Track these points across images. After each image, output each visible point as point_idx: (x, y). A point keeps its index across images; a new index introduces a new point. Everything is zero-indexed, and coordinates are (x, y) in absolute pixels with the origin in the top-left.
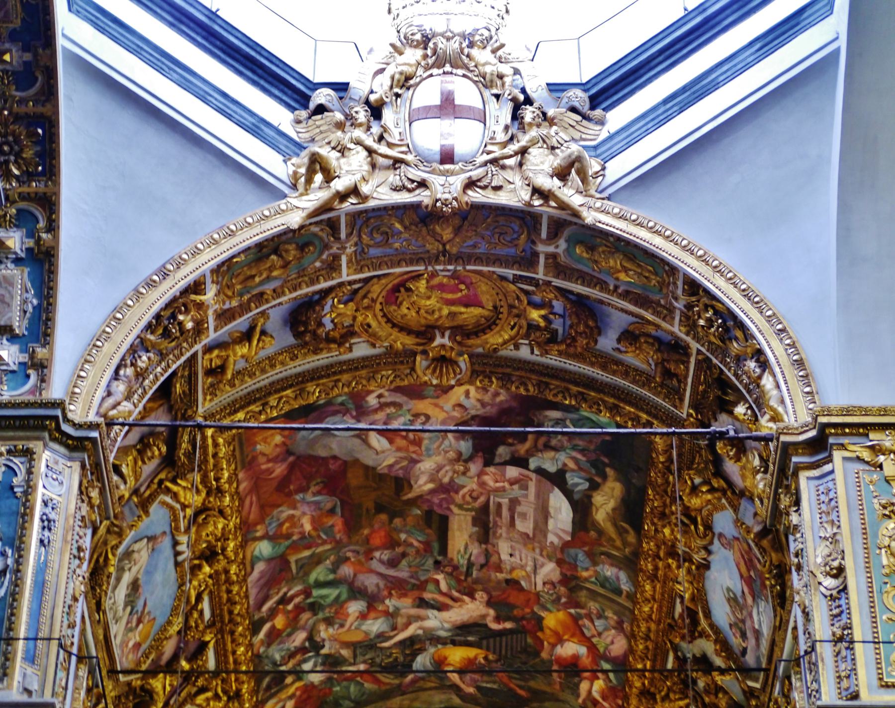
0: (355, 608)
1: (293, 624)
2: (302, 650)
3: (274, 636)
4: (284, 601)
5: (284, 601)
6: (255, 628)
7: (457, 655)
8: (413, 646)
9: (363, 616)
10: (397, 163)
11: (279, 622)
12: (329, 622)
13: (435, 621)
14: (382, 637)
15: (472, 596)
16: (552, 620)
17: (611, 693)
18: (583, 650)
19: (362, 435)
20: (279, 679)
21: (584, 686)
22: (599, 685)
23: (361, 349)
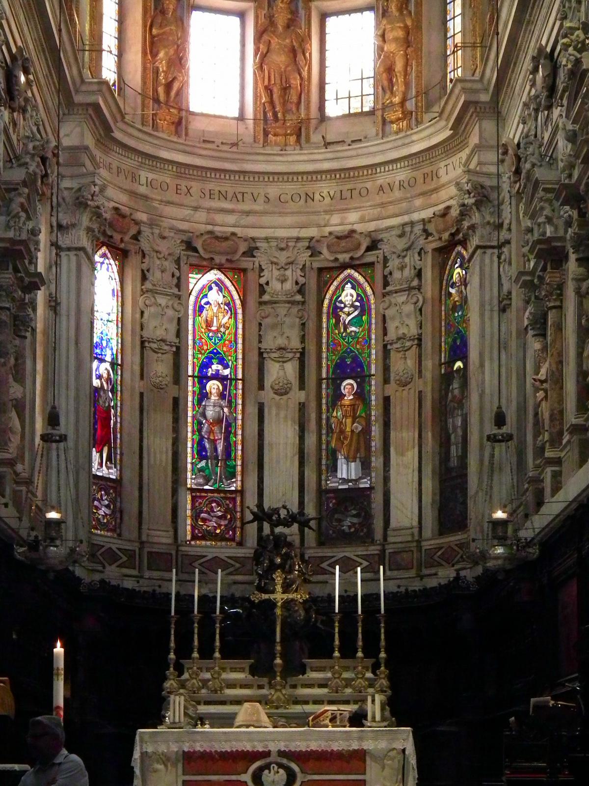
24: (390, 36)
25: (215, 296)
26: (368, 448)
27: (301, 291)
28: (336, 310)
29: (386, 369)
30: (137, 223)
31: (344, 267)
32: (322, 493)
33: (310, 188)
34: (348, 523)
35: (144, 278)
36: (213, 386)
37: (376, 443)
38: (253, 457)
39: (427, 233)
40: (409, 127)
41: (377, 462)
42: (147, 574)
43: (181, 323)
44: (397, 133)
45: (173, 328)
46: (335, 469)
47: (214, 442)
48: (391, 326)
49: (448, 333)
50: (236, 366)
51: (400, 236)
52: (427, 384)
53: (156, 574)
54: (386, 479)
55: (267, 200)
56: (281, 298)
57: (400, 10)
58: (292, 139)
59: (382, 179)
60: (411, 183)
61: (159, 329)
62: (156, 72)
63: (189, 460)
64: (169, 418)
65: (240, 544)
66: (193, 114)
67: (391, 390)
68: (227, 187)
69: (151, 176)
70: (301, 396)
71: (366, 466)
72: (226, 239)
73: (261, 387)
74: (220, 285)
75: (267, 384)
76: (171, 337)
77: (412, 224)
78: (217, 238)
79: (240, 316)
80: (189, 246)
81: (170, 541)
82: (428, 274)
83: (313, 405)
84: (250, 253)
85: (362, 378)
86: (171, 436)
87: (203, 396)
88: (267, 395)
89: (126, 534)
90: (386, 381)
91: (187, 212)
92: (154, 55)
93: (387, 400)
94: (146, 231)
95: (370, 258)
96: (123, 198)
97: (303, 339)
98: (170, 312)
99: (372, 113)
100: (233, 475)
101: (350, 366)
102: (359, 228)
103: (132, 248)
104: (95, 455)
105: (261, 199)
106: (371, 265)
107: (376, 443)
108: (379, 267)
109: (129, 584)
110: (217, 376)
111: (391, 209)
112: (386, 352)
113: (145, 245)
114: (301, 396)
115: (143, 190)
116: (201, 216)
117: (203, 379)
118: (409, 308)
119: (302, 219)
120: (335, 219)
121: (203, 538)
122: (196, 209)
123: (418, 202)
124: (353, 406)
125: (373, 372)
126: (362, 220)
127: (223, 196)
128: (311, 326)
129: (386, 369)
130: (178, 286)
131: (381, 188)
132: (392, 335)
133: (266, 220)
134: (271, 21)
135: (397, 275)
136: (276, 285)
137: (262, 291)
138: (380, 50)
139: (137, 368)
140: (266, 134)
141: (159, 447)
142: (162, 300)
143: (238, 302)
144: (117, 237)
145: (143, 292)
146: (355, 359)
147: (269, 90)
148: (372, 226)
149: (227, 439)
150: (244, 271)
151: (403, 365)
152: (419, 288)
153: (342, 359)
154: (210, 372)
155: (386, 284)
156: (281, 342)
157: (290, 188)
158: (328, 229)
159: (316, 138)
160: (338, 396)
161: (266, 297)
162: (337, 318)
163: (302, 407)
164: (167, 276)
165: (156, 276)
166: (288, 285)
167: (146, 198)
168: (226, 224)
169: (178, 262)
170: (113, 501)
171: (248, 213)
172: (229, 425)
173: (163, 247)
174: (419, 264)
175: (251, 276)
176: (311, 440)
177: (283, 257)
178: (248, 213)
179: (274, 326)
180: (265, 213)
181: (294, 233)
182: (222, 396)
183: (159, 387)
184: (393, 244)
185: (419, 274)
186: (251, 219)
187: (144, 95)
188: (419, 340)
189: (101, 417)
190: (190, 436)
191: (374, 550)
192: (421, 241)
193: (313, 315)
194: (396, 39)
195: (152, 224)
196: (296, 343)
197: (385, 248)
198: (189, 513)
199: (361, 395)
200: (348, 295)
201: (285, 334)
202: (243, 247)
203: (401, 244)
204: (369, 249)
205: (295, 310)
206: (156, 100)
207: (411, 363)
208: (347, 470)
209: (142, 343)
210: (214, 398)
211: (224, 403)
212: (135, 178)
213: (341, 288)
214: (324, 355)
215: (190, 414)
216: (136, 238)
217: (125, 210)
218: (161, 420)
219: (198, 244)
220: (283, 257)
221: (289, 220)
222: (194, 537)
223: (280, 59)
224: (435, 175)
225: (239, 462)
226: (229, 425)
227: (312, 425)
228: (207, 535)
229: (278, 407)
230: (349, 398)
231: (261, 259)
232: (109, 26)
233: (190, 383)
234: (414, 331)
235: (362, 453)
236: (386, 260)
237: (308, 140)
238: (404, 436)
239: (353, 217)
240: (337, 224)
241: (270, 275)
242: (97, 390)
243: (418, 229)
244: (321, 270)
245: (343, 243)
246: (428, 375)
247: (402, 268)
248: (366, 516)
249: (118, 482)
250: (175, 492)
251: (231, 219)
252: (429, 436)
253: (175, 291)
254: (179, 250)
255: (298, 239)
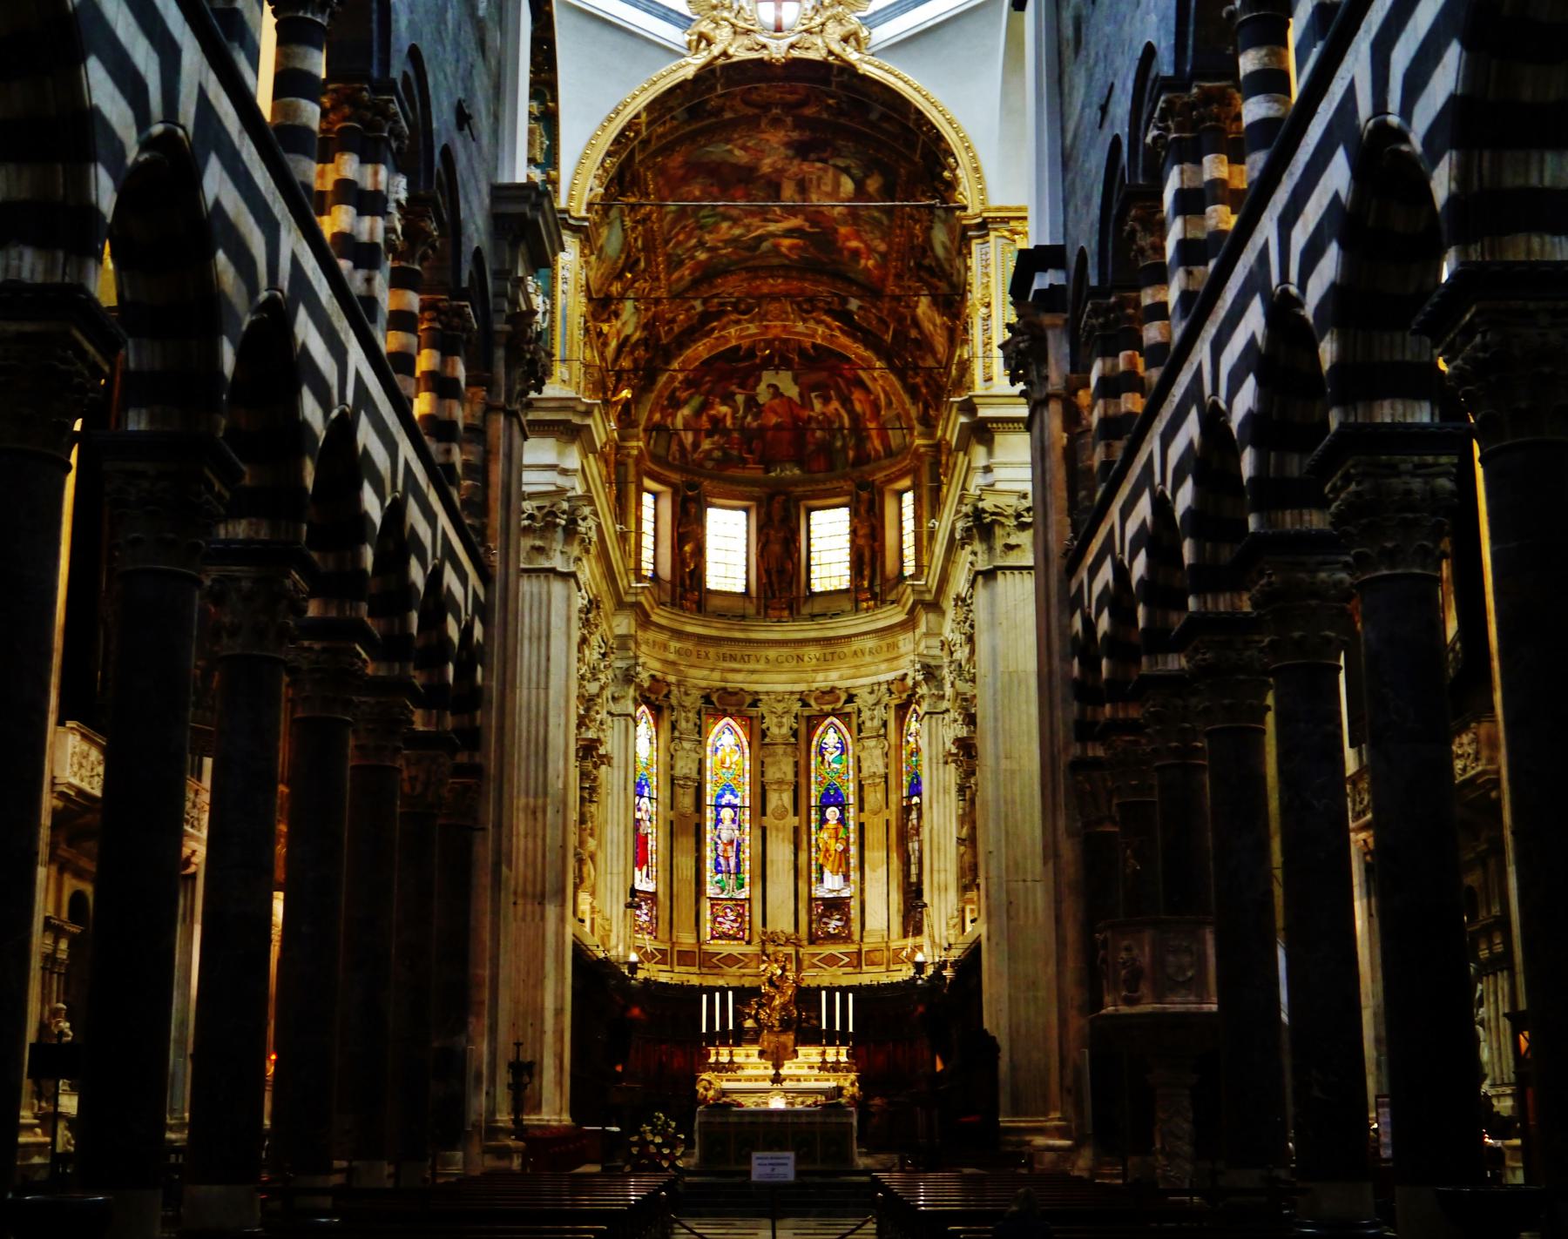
0: (725, 225)
1: (689, 237)
2: (695, 247)
3: (679, 244)
4: (684, 227)
5: (684, 227)
6: (667, 242)
7: (787, 242)
8: (761, 239)
9: (730, 228)
10: (747, 32)
11: (681, 237)
12: (710, 232)
13: (772, 227)
14: (742, 235)
15: (795, 216)
16: (843, 230)
17: (877, 266)
18: (861, 245)
19: (730, 151)
20: (681, 263)
21: (863, 262)
22: (871, 263)
23: (728, 115)
24: (861, 532)
25: (728, 740)
26: (848, 864)
27: (795, 734)
28: (821, 751)
29: (861, 800)
30: (668, 685)
31: (827, 715)
32: (811, 899)
33: (800, 651)
34: (834, 925)
35: (673, 727)
36: (727, 814)
37: (854, 861)
38: (758, 871)
39: (890, 692)
40: (876, 606)
41: (854, 876)
42: (677, 969)
43: (701, 764)
44: (867, 609)
45: (695, 767)
46: (822, 881)
47: (727, 859)
48: (865, 765)
49: (908, 773)
50: (744, 796)
51: (872, 692)
52: (892, 815)
53: (683, 969)
54: (862, 891)
55: (768, 661)
56: (779, 740)
57: (868, 512)
58: (786, 613)
59: (856, 645)
60: (878, 651)
61: (685, 767)
62: (684, 563)
63: (708, 874)
64: (693, 840)
65: (749, 943)
66: (710, 592)
67: (864, 817)
68: (736, 650)
69: (678, 645)
70: (795, 821)
71: (846, 878)
72: (736, 694)
73: (764, 813)
74: (732, 731)
75: (769, 811)
76: (694, 775)
77: (879, 684)
78: (731, 694)
79: (747, 755)
80: (707, 699)
81: (693, 941)
82: (892, 725)
83: (804, 828)
84: (755, 704)
85: (842, 806)
86: (694, 855)
87: (718, 821)
88: (768, 821)
89: (660, 936)
90: (861, 809)
91: (706, 673)
92: (681, 548)
93: (861, 828)
94: (673, 688)
95: (848, 708)
96: (657, 665)
97: (796, 774)
98: (694, 755)
99: (847, 591)
100: (742, 886)
101: (832, 797)
102: (839, 684)
103: (665, 705)
104: (637, 873)
105: (763, 661)
106: (848, 715)
107: (854, 861)
108: (854, 717)
109: (663, 978)
110: (729, 805)
111: (863, 670)
112: (861, 787)
113: (674, 702)
114: (795, 821)
115: (672, 657)
116: (716, 675)
117: (718, 807)
118: (878, 752)
119: (794, 676)
120: (820, 677)
121: (720, 938)
122: (712, 670)
123: (883, 666)
124: (836, 830)
125: (851, 800)
126: (841, 678)
127: (733, 658)
128: (802, 763)
129: (861, 800)
130: (699, 733)
131: (855, 653)
132: (865, 773)
133: (767, 677)
134: (769, 515)
135: (868, 724)
136: (774, 730)
137: (764, 734)
138: (853, 542)
139: (668, 801)
140: (766, 607)
141: (685, 865)
142: (687, 745)
143: (746, 744)
144: (653, 697)
145: (673, 739)
146: (837, 790)
147: (768, 572)
148: (848, 683)
149: (737, 856)
150: (751, 718)
151: (874, 798)
152: (885, 736)
153: (827, 790)
154: (724, 801)
155: (860, 731)
156: (778, 775)
157: (785, 651)
158: (815, 685)
159: (805, 610)
160: (823, 821)
161: (767, 740)
162: (823, 756)
163: (796, 830)
164: (691, 725)
165: (683, 725)
166: (785, 730)
167: (673, 663)
168: (738, 681)
169: (699, 713)
170: (651, 910)
171: (753, 672)
172: (739, 845)
173: (688, 702)
174: (885, 716)
175: (756, 723)
176: (803, 857)
177: (780, 708)
178: (753, 672)
179: (774, 764)
180: (765, 671)
181: (789, 688)
182: (733, 821)
183: (683, 815)
184: (864, 699)
185: (885, 724)
186: (755, 677)
187: (672, 582)
188: (886, 777)
189: (641, 842)
190: (709, 855)
191: (853, 948)
192: (886, 699)
193: (804, 753)
194: (865, 536)
195: (679, 684)
196: (790, 777)
197: (859, 702)
198: (709, 917)
199: (842, 821)
200: (831, 739)
201: (782, 769)
202: (749, 700)
203: (872, 699)
204: (846, 702)
205: (789, 749)
206: (683, 585)
207: (880, 796)
208: (832, 884)
209: (673, 779)
210: (727, 822)
211: (735, 826)
212: (665, 647)
213: (825, 732)
214: (813, 787)
215: (708, 836)
216: (667, 696)
217: (659, 675)
218: (687, 843)
219: (714, 699)
220: (780, 708)
221: (784, 677)
222: (713, 938)
223: (776, 548)
224: (895, 646)
225: (747, 875)
226: (739, 845)
227: (804, 845)
228: (724, 936)
229: (777, 829)
230: (833, 823)
231: (763, 709)
232: (648, 527)
233: (708, 810)
234: (882, 770)
235: (843, 868)
236: (860, 711)
237: (799, 613)
238: (875, 855)
239: (834, 675)
240: (822, 680)
241: (770, 721)
242: (638, 821)
243: (884, 687)
244: (809, 718)
245: (827, 697)
246: (893, 806)
247: (872, 719)
248: (847, 922)
249: (655, 894)
250: (698, 902)
251: (739, 677)
252: (894, 856)
253: (696, 737)
254: (699, 703)
255: (792, 693)
